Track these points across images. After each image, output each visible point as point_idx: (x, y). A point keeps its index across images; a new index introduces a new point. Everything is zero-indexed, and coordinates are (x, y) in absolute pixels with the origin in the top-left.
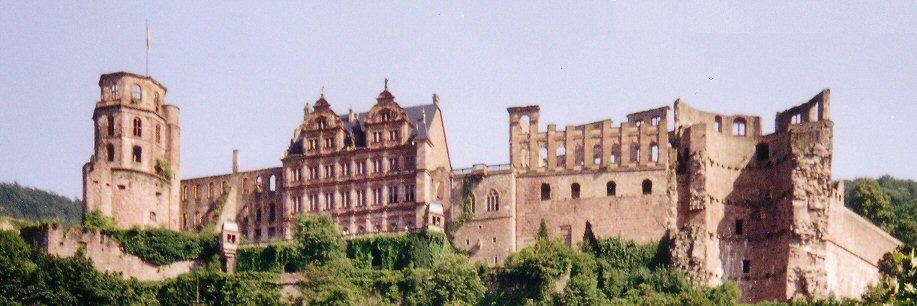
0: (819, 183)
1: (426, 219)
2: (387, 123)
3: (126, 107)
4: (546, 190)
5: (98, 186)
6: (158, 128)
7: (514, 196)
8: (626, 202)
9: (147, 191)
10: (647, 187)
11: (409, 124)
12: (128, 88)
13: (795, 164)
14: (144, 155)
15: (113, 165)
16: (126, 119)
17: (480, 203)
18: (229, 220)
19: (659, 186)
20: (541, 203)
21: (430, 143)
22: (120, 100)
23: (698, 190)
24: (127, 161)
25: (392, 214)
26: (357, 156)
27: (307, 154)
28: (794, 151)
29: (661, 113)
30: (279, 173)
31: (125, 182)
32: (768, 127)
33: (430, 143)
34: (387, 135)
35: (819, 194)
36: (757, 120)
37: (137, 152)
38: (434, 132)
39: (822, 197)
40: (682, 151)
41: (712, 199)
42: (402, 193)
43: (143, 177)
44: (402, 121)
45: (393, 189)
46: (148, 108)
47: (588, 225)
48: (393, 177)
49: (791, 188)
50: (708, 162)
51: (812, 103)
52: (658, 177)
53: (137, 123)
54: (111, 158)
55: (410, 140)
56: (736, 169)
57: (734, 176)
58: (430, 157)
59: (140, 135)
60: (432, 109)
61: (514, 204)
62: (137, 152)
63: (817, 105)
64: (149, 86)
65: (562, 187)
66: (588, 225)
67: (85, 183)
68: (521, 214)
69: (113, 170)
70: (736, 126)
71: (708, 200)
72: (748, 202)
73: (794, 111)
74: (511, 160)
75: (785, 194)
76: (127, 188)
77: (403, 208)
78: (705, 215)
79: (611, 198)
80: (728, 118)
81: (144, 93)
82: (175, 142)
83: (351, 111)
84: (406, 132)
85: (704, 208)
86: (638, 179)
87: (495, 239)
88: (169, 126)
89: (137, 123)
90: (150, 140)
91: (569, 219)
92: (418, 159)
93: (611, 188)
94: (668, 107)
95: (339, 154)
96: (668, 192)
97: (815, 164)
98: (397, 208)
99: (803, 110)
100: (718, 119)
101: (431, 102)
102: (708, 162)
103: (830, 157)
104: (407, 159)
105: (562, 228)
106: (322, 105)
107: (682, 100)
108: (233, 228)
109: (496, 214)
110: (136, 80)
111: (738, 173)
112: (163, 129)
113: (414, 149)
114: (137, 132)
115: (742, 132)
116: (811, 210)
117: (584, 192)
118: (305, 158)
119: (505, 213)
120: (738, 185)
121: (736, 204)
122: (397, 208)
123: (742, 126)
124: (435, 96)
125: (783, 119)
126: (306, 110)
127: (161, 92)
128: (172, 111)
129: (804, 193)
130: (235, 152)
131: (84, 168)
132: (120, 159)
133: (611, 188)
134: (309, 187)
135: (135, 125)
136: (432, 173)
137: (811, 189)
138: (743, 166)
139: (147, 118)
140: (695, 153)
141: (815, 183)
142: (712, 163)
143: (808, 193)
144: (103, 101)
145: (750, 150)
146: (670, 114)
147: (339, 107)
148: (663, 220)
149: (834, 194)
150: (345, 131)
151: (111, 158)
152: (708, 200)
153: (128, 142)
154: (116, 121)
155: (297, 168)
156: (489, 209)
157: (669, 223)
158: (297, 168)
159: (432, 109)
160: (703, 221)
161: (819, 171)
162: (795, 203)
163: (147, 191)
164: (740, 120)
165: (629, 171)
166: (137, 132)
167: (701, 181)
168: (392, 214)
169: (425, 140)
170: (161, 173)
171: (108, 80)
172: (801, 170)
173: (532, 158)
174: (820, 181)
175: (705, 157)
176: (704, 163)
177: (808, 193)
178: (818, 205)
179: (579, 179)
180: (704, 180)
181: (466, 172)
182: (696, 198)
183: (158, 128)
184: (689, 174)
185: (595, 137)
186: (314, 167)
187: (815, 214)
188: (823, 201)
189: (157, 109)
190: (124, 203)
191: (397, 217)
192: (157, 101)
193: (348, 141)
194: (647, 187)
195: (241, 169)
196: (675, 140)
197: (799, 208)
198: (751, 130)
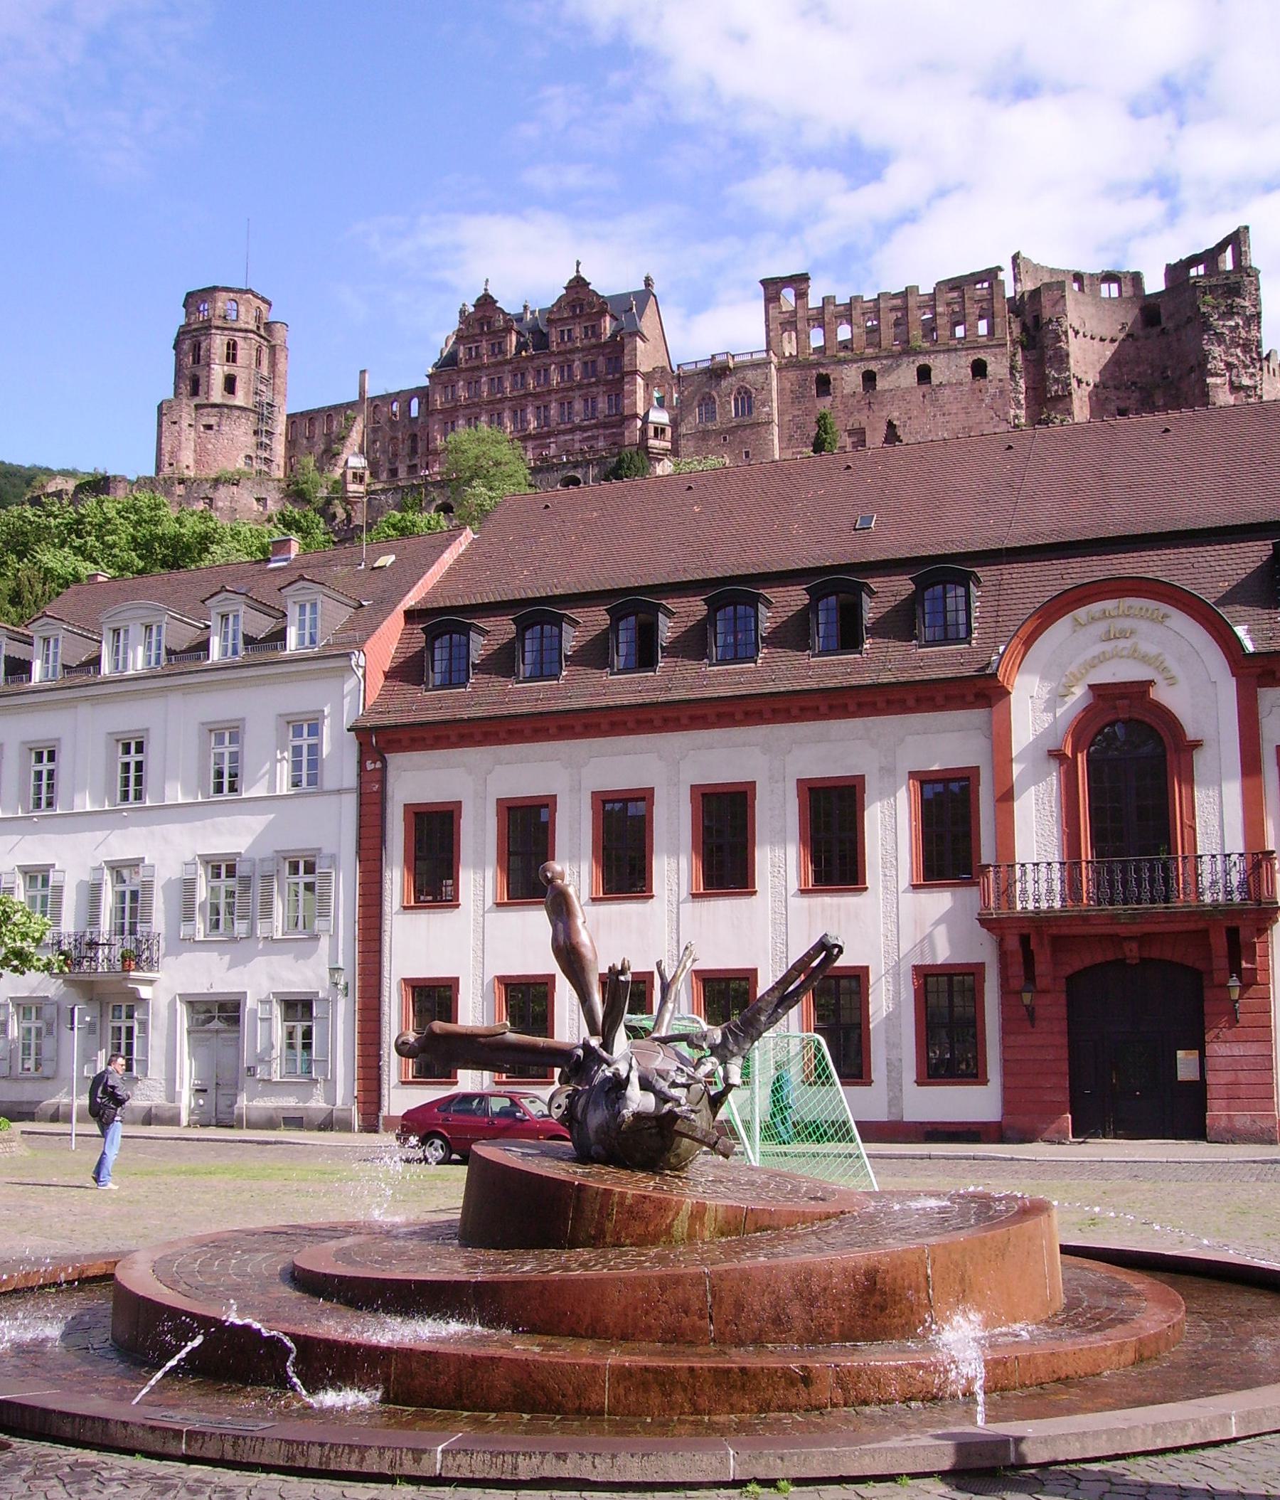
0: (1244, 352)
1: (644, 431)
2: (578, 316)
3: (217, 328)
4: (824, 384)
5: (176, 427)
6: (259, 350)
7: (775, 395)
8: (947, 391)
9: (242, 430)
10: (979, 369)
11: (612, 316)
12: (222, 303)
13: (1207, 327)
14: (239, 385)
15: (197, 400)
16: (218, 343)
17: (722, 406)
18: (354, 454)
19: (997, 367)
20: (817, 400)
21: (644, 339)
22: (210, 320)
23: (1059, 371)
24: (217, 395)
25: (589, 434)
26: (537, 362)
27: (463, 366)
28: (1203, 310)
29: (991, 275)
30: (422, 393)
31: (213, 421)
32: (1154, 283)
33: (644, 339)
34: (578, 332)
35: (1246, 367)
36: (1136, 278)
37: (230, 384)
38: (647, 324)
39: (1251, 370)
40: (1029, 321)
41: (1079, 381)
42: (602, 404)
43: (237, 413)
44: (602, 313)
45: (590, 402)
46: (246, 326)
47: (891, 425)
48: (590, 385)
49: (1204, 358)
50: (1071, 333)
51: (1221, 247)
52: (995, 355)
53: (232, 346)
54: (195, 392)
55: (613, 336)
56: (1113, 341)
57: (1109, 351)
58: (645, 357)
59: (234, 361)
60: (646, 295)
61: (775, 405)
62: (230, 384)
63: (1229, 249)
64: (248, 301)
65: (849, 378)
66: (891, 425)
67: (160, 425)
68: (787, 418)
69: (198, 407)
70: (1104, 287)
71: (1074, 383)
72: (1134, 383)
73: (1193, 261)
74: (768, 343)
75: (1192, 369)
76: (215, 428)
77: (605, 426)
78: (1071, 402)
79: (925, 388)
80: (1092, 275)
81: (242, 309)
82: (281, 367)
83: (525, 307)
84: (608, 325)
85: (1070, 394)
86: (966, 360)
87: (747, 453)
88: (273, 349)
89: (232, 346)
90: (248, 367)
91: (861, 419)
92: (626, 358)
93: (924, 374)
94: (999, 269)
95: (510, 362)
96: (1011, 374)
97: (1237, 325)
98: (596, 426)
99: (1210, 257)
100: (1078, 277)
101: (643, 287)
102: (1071, 333)
103: (1259, 315)
104: (612, 364)
105: (851, 433)
106: (486, 302)
107: (1023, 254)
108: (358, 462)
109: (747, 420)
110: (232, 295)
111: (1116, 344)
112: (265, 351)
113: (622, 346)
114: (231, 357)
115: (1115, 294)
116: (1235, 388)
117: (881, 384)
118: (461, 371)
119: (763, 418)
120: (1116, 362)
121: (1116, 388)
122: (596, 426)
123: (1114, 287)
124: (648, 282)
125: (1176, 272)
126: (462, 312)
127: (264, 307)
128: (279, 331)
129: (1222, 365)
130: (363, 372)
131: (160, 407)
132: (207, 393)
133: (924, 374)
134: (467, 407)
135: (228, 348)
136: (646, 376)
137: (1230, 360)
138: (1122, 336)
139: (245, 338)
140: (1050, 321)
141: (1238, 350)
142: (1077, 333)
143: (1229, 366)
144: (188, 324)
145: (1130, 315)
146: (1006, 276)
147: (509, 303)
148: (1008, 412)
149: (1265, 369)
150: (518, 333)
151: (195, 392)
152: (1074, 383)
153: (218, 372)
154: (204, 345)
155: (449, 385)
156: (737, 414)
157: (1016, 417)
158: (449, 385)
159: (646, 295)
160: (1070, 413)
161: (1243, 334)
162: (1210, 380)
163: (242, 430)
164: (1109, 277)
165: (948, 350)
166: (231, 357)
167: (1062, 359)
168: (589, 434)
169: (638, 333)
170: (262, 413)
171: (194, 300)
172: (1216, 334)
173: (802, 342)
174: (1246, 348)
175: (1066, 324)
176: (1066, 333)
177: (1229, 366)
178: (1246, 381)
179: (874, 366)
180: (1068, 355)
181: (700, 366)
182: (1057, 381)
183: (259, 350)
184: (1043, 349)
185: (893, 309)
186: (473, 384)
187: (1242, 394)
188: (1253, 375)
189: (258, 328)
190: (210, 446)
191: (595, 438)
192: (258, 318)
193: (521, 346)
194: (979, 369)
195: (371, 392)
196: (1016, 307)
197: (1216, 386)
198: (1128, 291)
